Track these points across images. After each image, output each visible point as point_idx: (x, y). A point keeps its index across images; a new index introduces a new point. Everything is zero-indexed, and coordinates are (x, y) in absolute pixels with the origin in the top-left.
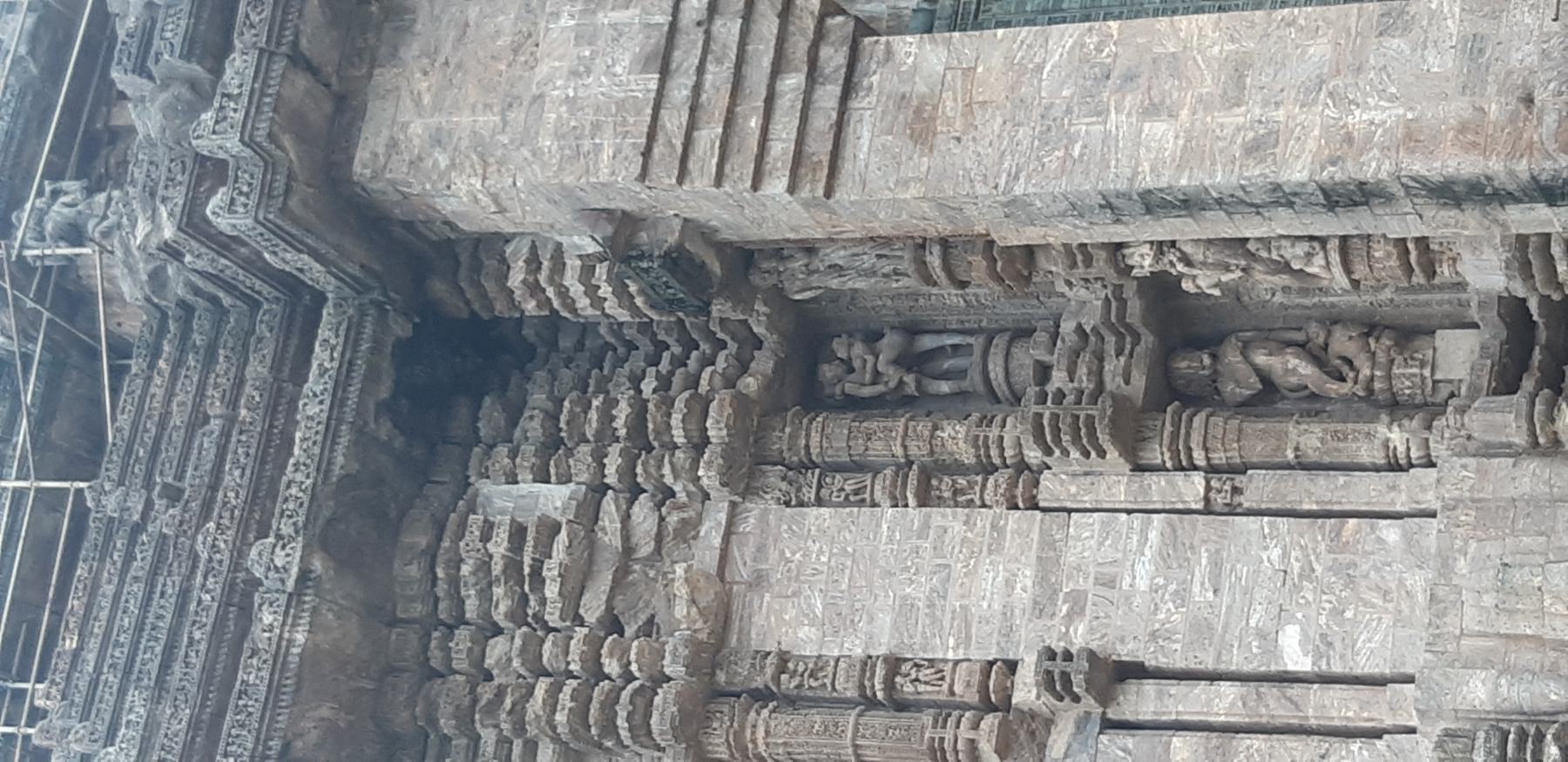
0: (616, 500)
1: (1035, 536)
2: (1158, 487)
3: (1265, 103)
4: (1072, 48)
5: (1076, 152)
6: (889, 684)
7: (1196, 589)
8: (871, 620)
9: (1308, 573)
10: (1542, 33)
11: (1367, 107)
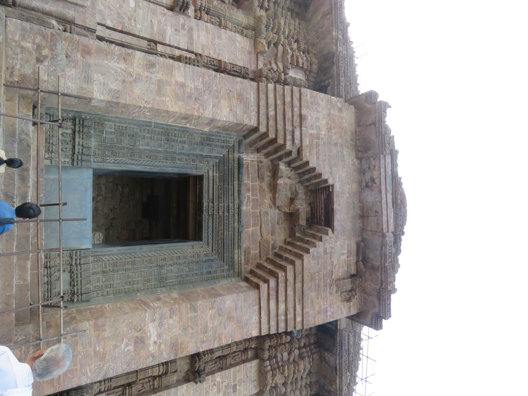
0: (280, 70)
1: (195, 46)
3: (151, 78)
4: (206, 109)
5: (201, 79)
7: (156, 23)
8: (226, 37)
9: (130, 19)
10: (65, 78)
11: (121, 69)
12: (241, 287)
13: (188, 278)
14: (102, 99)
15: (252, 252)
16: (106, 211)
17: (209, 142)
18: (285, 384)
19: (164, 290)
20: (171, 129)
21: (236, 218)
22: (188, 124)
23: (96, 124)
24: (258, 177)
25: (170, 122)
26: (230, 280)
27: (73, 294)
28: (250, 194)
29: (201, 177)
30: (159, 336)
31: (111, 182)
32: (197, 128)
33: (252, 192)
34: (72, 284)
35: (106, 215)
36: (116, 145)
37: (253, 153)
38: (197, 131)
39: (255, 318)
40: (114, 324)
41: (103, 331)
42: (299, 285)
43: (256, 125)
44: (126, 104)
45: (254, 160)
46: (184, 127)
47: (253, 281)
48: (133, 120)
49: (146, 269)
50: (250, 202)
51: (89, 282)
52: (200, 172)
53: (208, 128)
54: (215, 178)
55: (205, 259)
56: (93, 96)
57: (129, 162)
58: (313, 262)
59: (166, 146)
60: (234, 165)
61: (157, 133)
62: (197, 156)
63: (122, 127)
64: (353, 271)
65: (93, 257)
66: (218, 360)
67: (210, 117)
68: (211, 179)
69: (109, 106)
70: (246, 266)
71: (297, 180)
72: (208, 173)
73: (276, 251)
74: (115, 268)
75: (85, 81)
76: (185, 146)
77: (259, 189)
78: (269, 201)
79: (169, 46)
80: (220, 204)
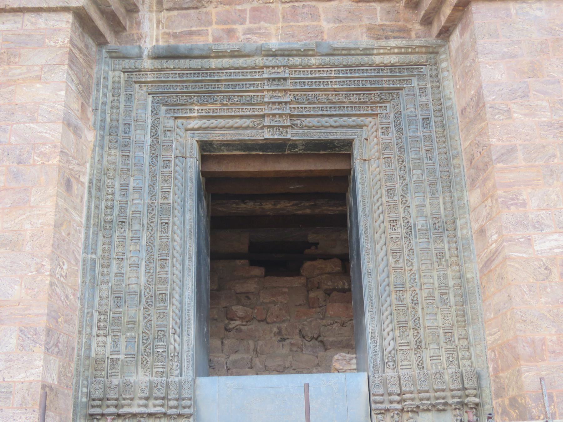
12: (462, 45)
13: (438, 168)
14: (42, 363)
15: (379, 22)
16: (285, 351)
17: (121, 128)
19: (463, 221)
20: (97, 216)
21: (297, 60)
22: (82, 179)
23: (99, 373)
24: (197, 8)
26: (446, 73)
27: (463, 404)
28: (240, 28)
29: (205, 146)
31: (222, 343)
32: (89, 158)
33: (234, 23)
34: (440, 407)
35: (295, 349)
36: (141, 332)
37: (139, 24)
38: (97, 159)
40: (531, 322)
41: (544, 344)
43: (69, 17)
44: (48, 315)
45: (155, 20)
46: (90, 188)
47: (449, 16)
48: (82, 299)
49: (415, 260)
50: (260, 28)
51: (439, 375)
52: (192, 149)
53: (86, 131)
54: (204, 114)
55: (393, 133)
56: (38, 381)
57: (176, 303)
59: (136, 227)
60: (171, 70)
61: (107, 247)
62: (154, 157)
63: (99, 321)
65: (387, 370)
67: (59, 127)
69: (56, 350)
70: (413, 34)
72: (193, 129)
74: (411, 324)
75: (7, 398)
76: (132, 184)
77: (227, 7)
80: (266, 100)
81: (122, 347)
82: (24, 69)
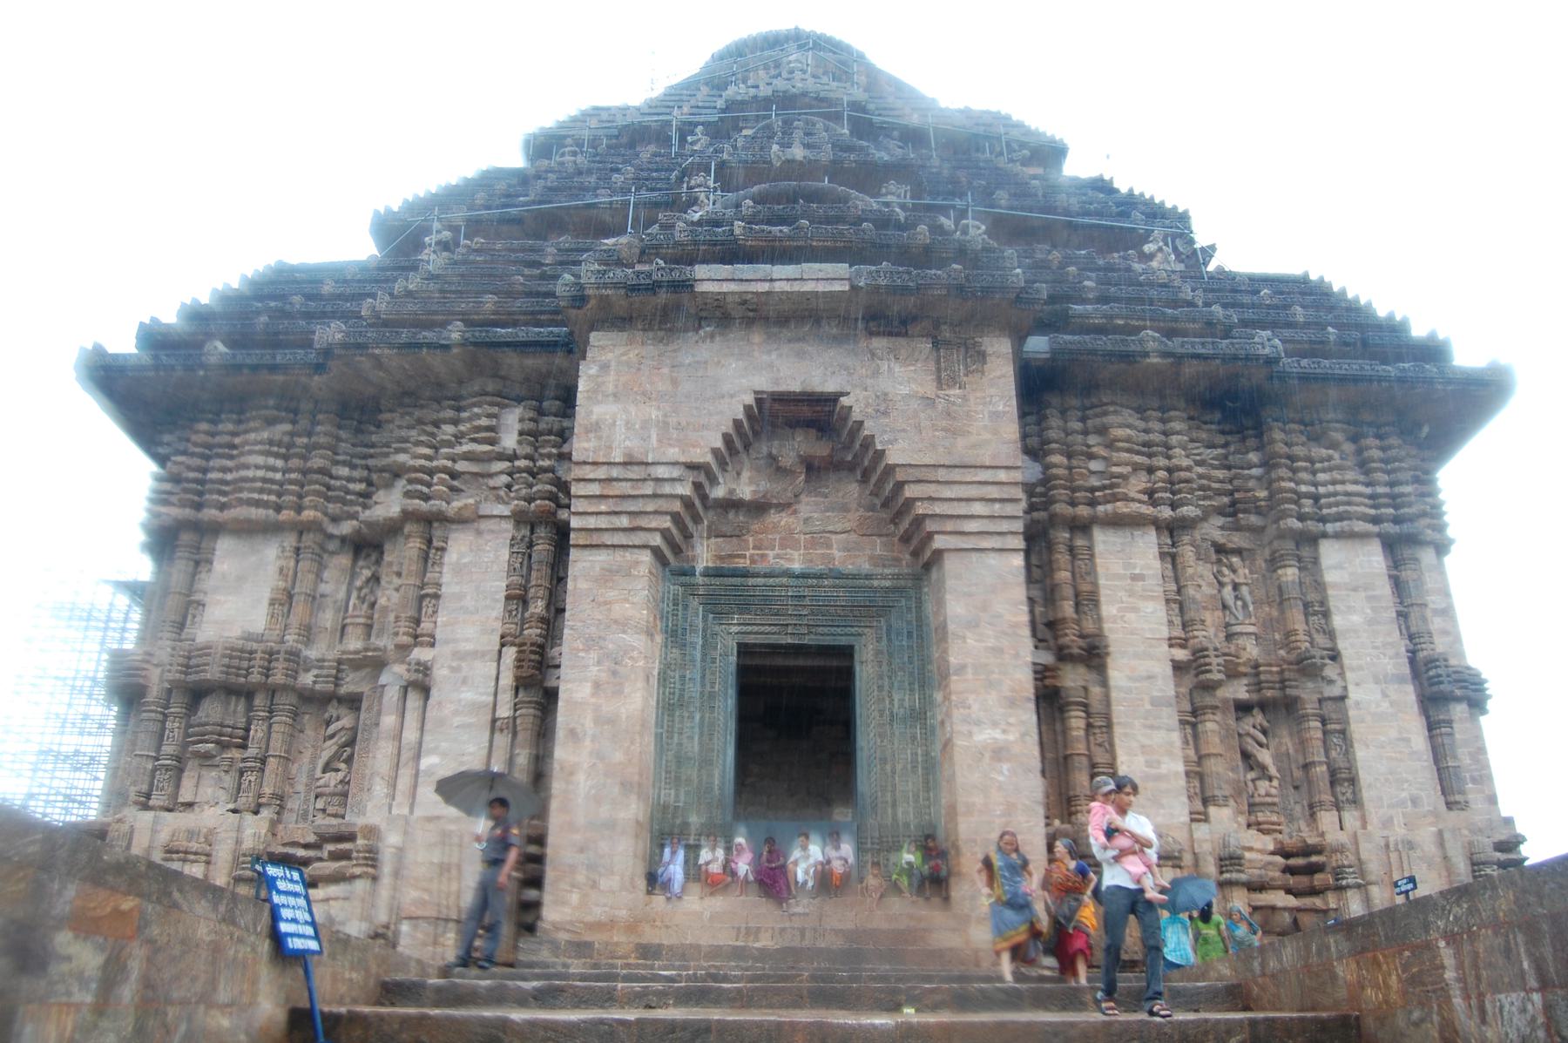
2: (506, 698)
5: (582, 654)
6: (427, 595)
8: (457, 583)
15: (878, 552)
18: (1151, 470)
25: (654, 703)
30: (995, 724)
37: (693, 547)
39: (993, 560)
42: (942, 474)
55: (884, 642)
58: (901, 444)
62: (704, 655)
64: (926, 346)
66: (1081, 608)
68: (745, 628)
71: (743, 456)
73: (878, 502)
74: (890, 788)
76: (688, 676)
78: (783, 514)
79: (496, 694)
81: (682, 798)
82: (616, 592)
